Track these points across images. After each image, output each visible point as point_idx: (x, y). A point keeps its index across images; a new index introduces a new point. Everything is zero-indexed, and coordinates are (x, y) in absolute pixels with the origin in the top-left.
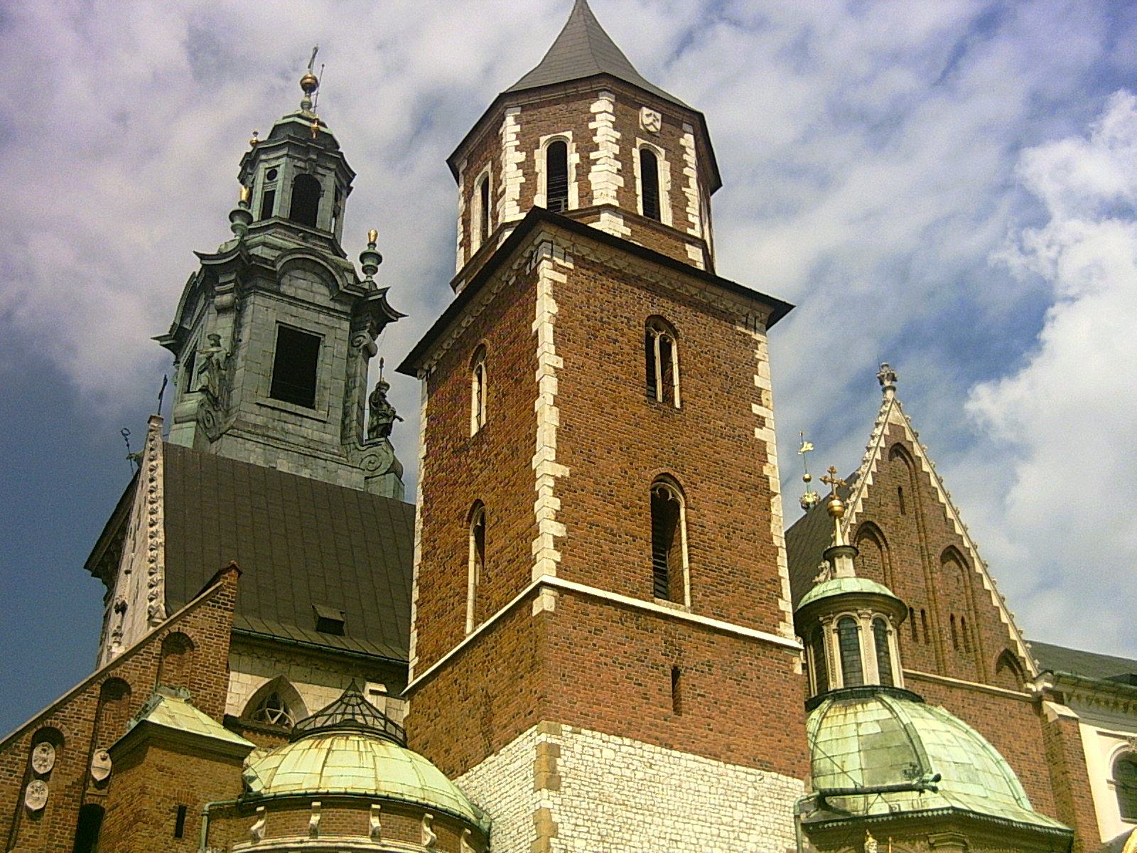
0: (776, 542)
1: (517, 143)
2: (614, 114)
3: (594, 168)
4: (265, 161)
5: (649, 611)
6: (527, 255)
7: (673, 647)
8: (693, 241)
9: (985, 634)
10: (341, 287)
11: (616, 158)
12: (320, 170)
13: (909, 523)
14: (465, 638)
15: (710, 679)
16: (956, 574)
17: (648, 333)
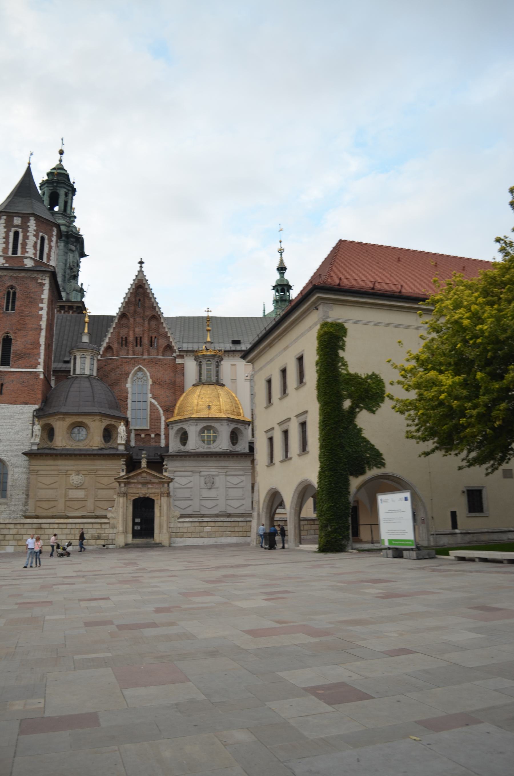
0: (41, 343)
2: (5, 223)
8: (26, 258)
9: (160, 341)
11: (4, 238)
12: (59, 189)
16: (155, 323)
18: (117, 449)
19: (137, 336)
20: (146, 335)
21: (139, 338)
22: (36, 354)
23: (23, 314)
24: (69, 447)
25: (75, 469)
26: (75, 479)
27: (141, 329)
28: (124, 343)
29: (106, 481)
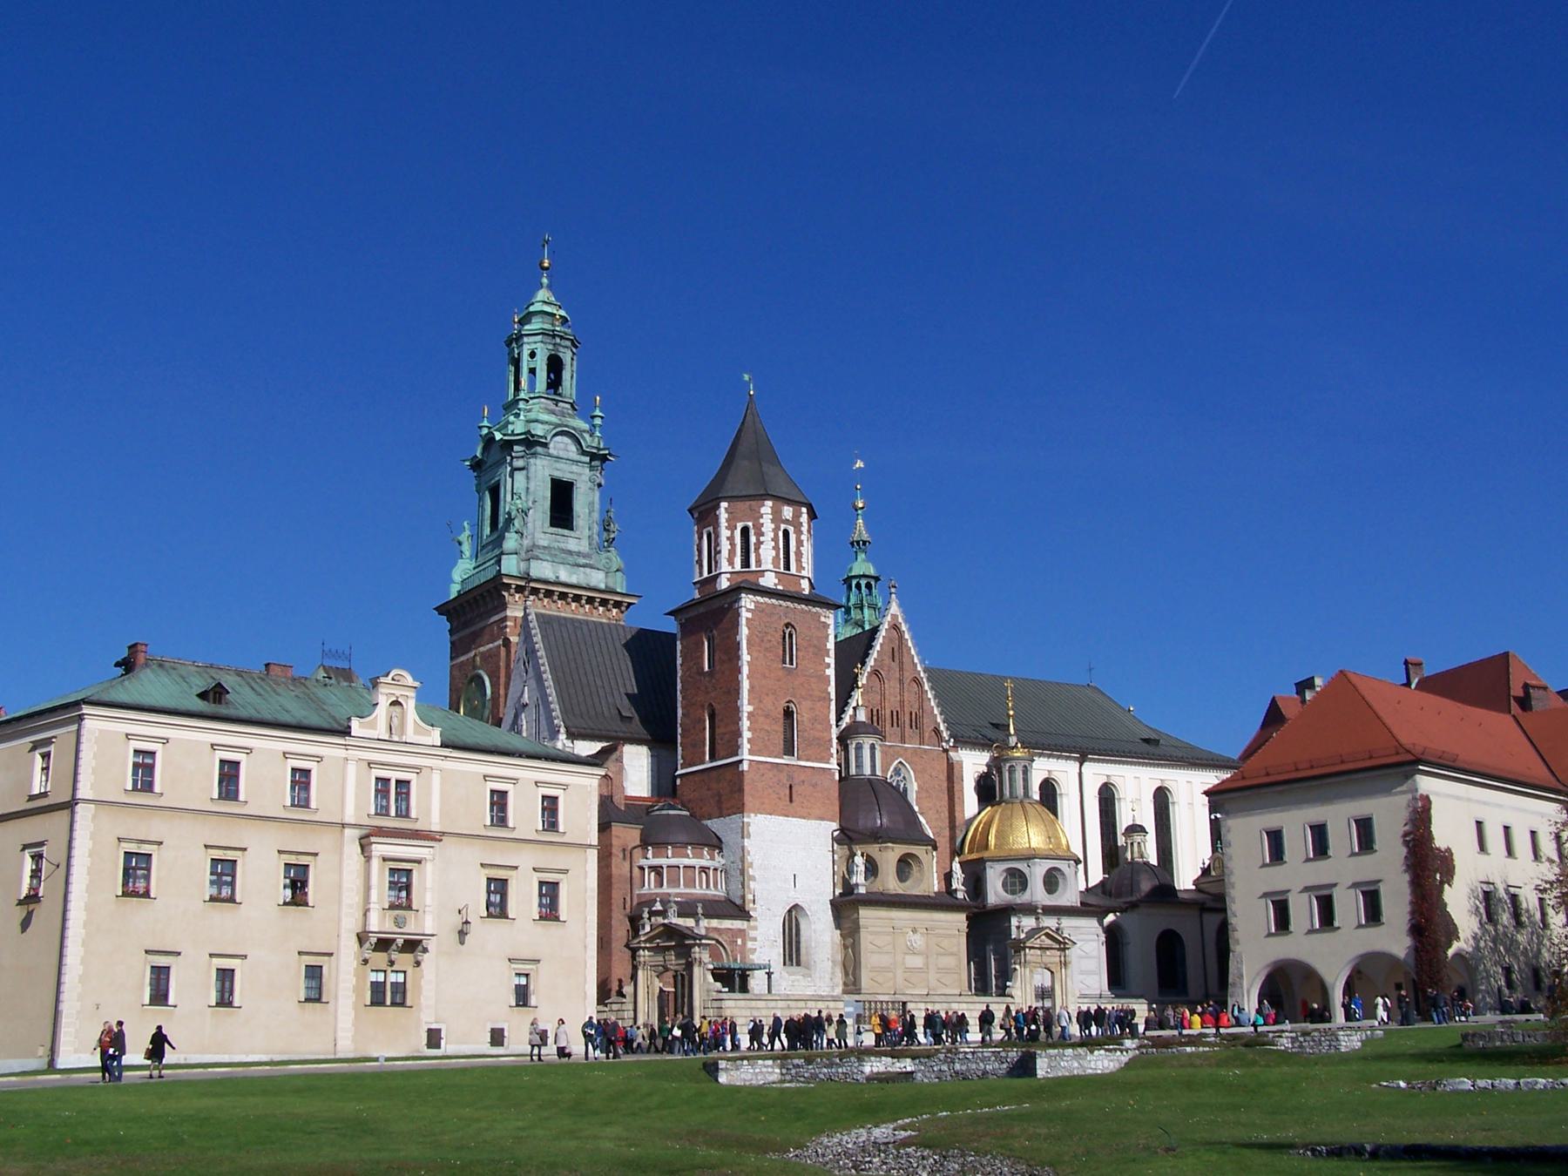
0: (831, 722)
1: (726, 524)
2: (772, 514)
3: (762, 546)
4: (528, 343)
5: (781, 764)
6: (734, 598)
7: (790, 777)
8: (803, 577)
10: (584, 448)
11: (772, 540)
12: (561, 349)
13: (895, 665)
14: (703, 762)
15: (803, 787)
17: (783, 631)
18: (957, 898)
19: (892, 709)
20: (907, 711)
21: (895, 713)
22: (827, 739)
23: (807, 673)
24: (901, 892)
25: (912, 926)
26: (918, 940)
27: (898, 698)
28: (875, 718)
29: (945, 943)
